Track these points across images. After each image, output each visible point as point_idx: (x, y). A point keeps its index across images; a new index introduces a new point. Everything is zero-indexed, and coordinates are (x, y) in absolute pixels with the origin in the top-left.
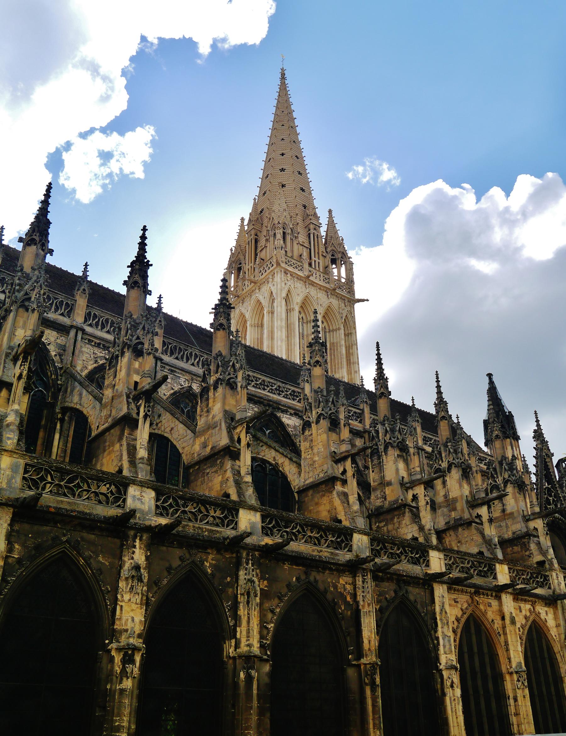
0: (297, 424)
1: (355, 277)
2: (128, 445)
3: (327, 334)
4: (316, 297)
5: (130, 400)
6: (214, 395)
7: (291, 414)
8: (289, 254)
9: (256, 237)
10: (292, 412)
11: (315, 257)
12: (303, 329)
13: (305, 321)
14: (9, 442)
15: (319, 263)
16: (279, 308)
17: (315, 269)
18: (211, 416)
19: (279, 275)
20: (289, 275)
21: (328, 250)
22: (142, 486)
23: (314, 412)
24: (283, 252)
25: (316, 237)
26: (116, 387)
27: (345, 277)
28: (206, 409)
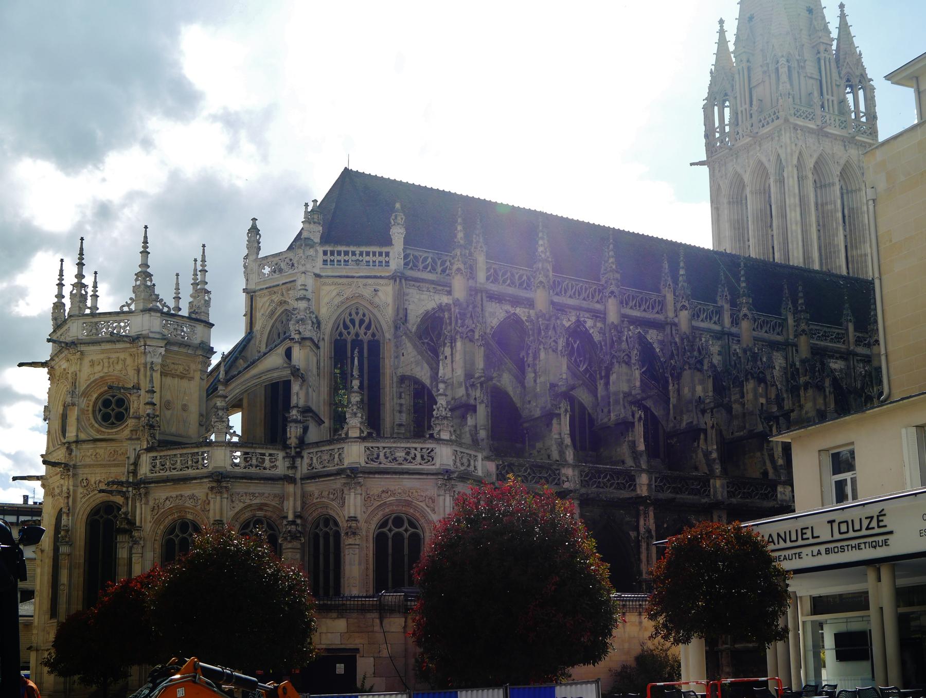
0: (843, 367)
1: (878, 109)
2: (769, 455)
3: (845, 196)
4: (831, 153)
5: (763, 420)
6: (805, 394)
7: (837, 358)
8: (797, 101)
9: (749, 64)
10: (838, 355)
11: (828, 94)
12: (816, 196)
13: (818, 185)
14: (717, 471)
15: (833, 101)
16: (791, 179)
17: (829, 113)
18: (804, 412)
19: (788, 134)
20: (799, 131)
21: (843, 73)
22: (784, 485)
23: (875, 389)
24: (791, 100)
25: (827, 63)
26: (746, 406)
27: (864, 111)
28: (797, 404)
